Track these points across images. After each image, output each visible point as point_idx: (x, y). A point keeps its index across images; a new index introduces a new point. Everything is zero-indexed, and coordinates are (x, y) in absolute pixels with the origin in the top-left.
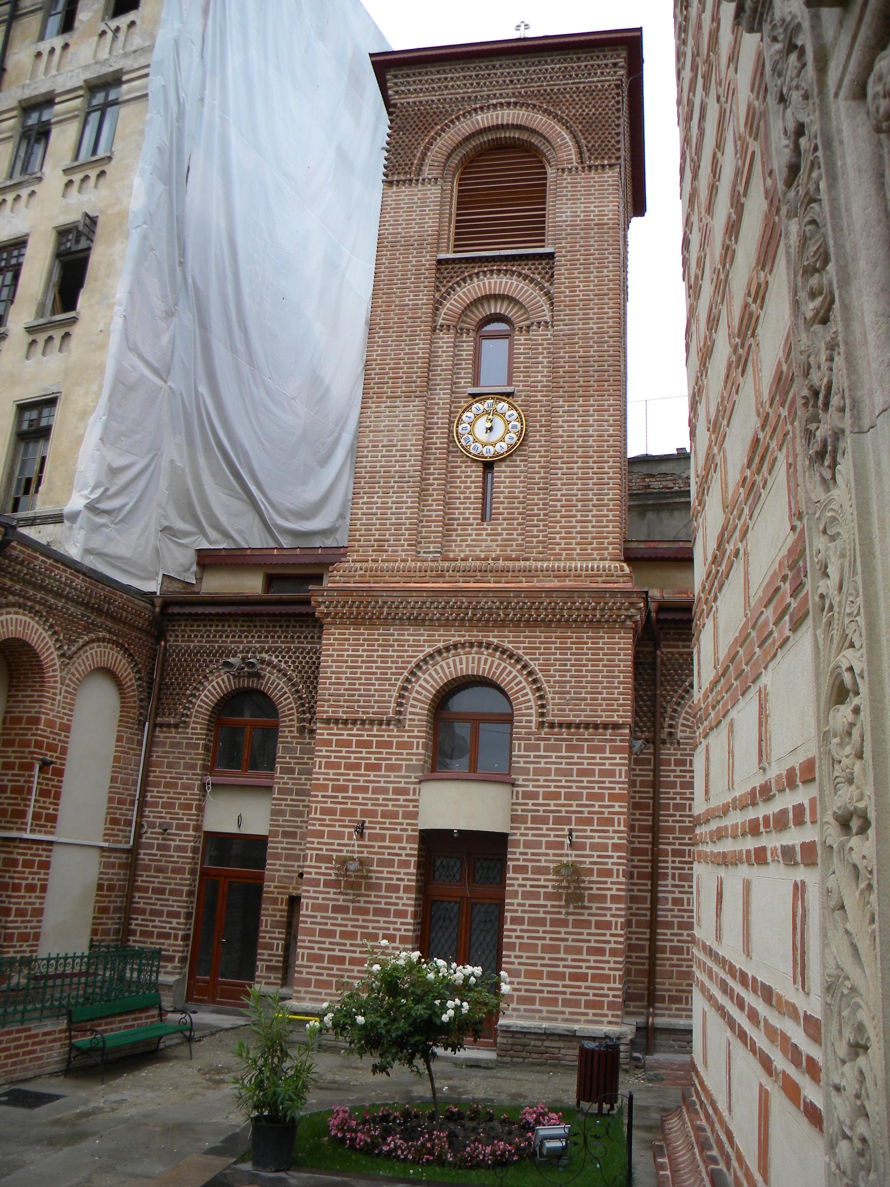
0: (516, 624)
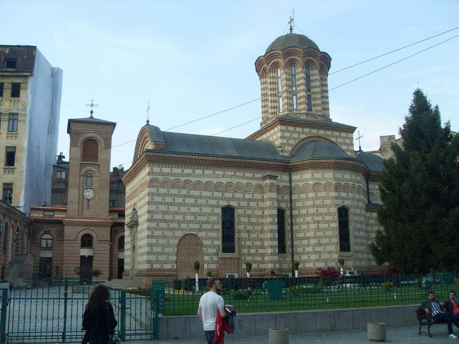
0: (94, 226)
